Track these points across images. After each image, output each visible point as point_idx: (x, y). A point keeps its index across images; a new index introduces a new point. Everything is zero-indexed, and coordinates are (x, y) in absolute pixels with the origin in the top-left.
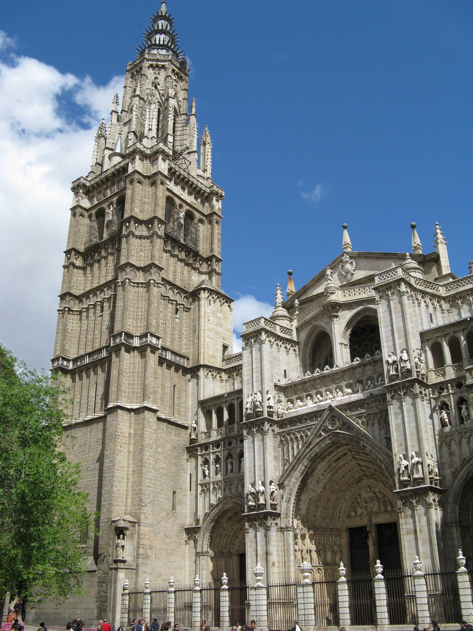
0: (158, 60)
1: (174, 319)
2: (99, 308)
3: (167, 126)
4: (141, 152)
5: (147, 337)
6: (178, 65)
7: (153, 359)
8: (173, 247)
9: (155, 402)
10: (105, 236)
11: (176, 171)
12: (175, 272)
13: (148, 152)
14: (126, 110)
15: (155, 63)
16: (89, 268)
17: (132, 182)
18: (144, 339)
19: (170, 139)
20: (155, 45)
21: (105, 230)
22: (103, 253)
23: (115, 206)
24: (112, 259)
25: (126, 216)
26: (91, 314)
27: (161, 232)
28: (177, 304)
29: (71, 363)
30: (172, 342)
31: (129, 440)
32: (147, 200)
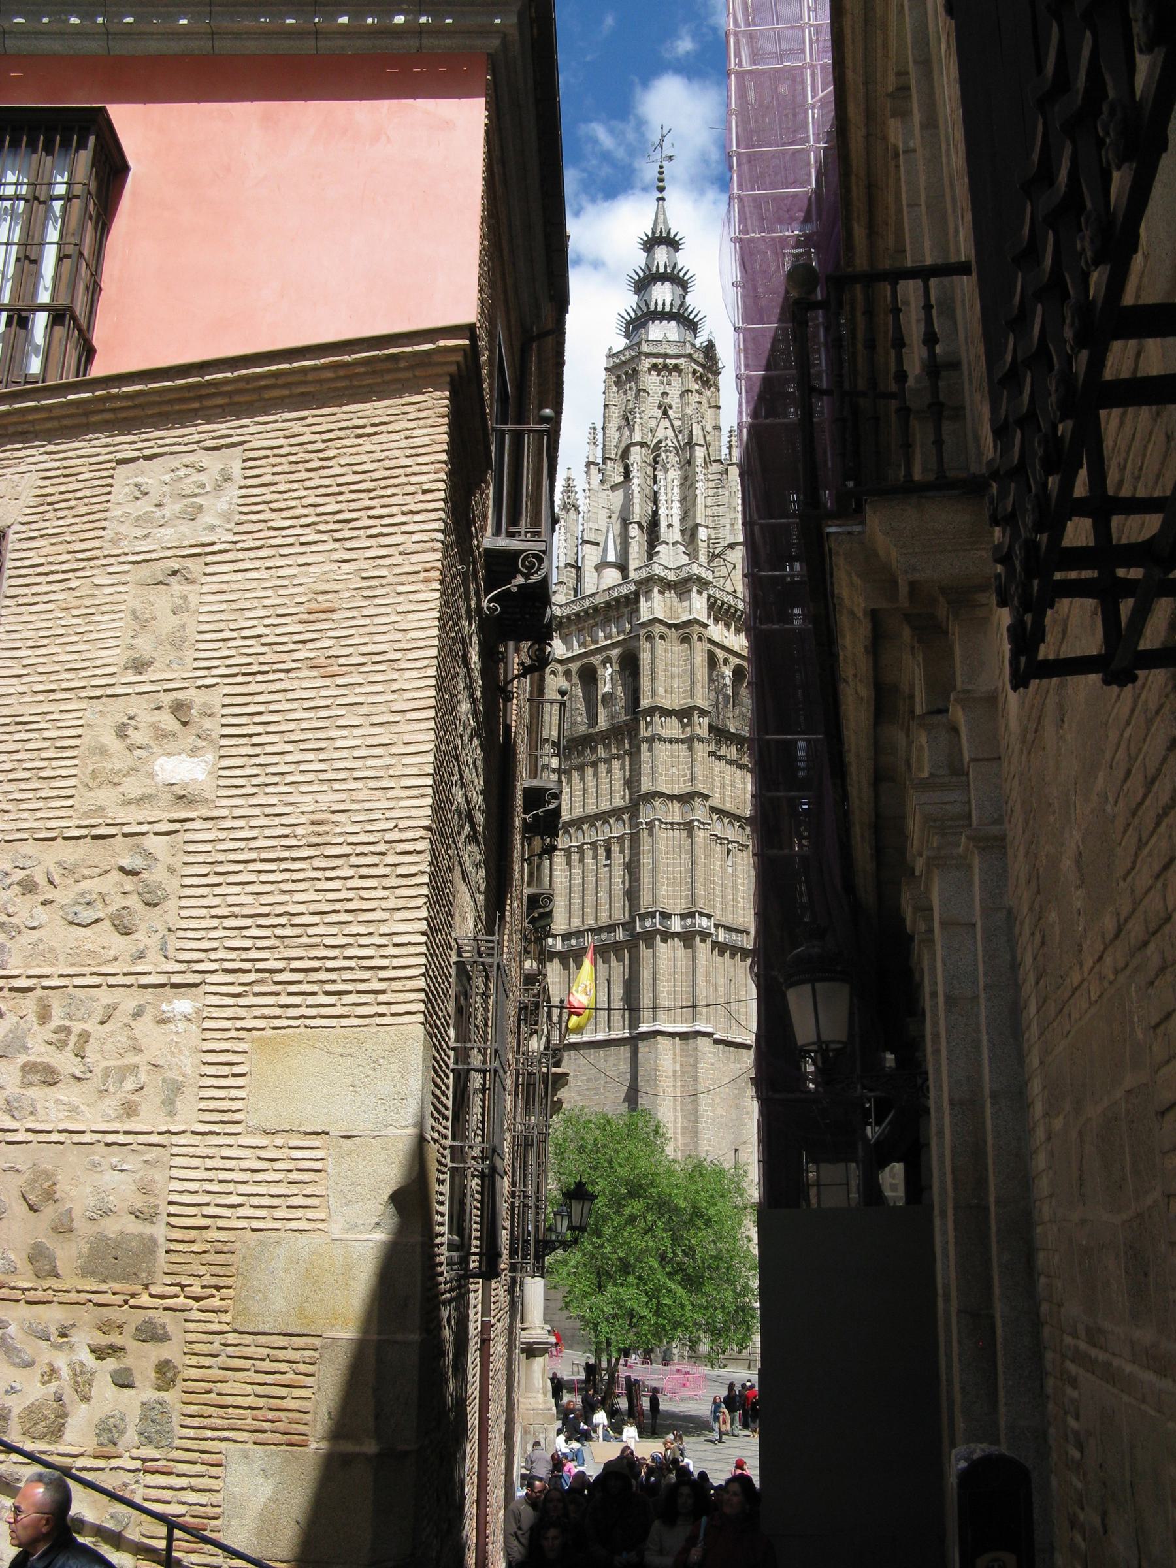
0: (666, 356)
1: (724, 868)
2: (601, 851)
3: (694, 504)
4: (661, 579)
5: (694, 917)
6: (700, 357)
7: (703, 949)
8: (718, 743)
9: (708, 1021)
10: (603, 723)
11: (716, 600)
12: (723, 787)
13: (671, 576)
14: (613, 456)
15: (661, 360)
16: (575, 774)
17: (649, 638)
18: (689, 921)
19: (702, 533)
20: (655, 312)
21: (601, 709)
22: (602, 753)
23: (616, 667)
24: (618, 766)
25: (645, 702)
26: (589, 860)
27: (703, 732)
28: (730, 842)
29: (559, 939)
30: (724, 910)
31: (675, 1081)
32: (675, 670)
